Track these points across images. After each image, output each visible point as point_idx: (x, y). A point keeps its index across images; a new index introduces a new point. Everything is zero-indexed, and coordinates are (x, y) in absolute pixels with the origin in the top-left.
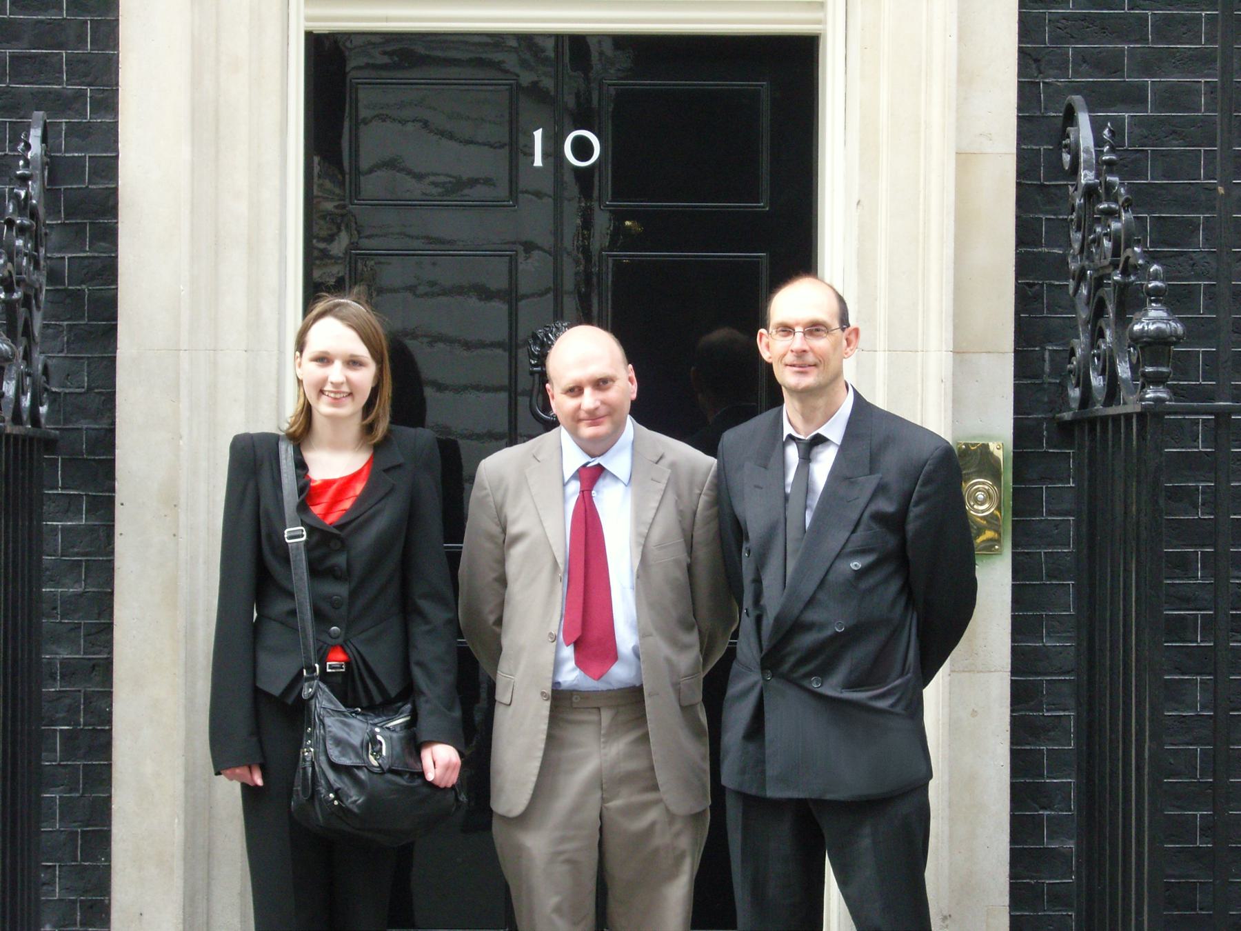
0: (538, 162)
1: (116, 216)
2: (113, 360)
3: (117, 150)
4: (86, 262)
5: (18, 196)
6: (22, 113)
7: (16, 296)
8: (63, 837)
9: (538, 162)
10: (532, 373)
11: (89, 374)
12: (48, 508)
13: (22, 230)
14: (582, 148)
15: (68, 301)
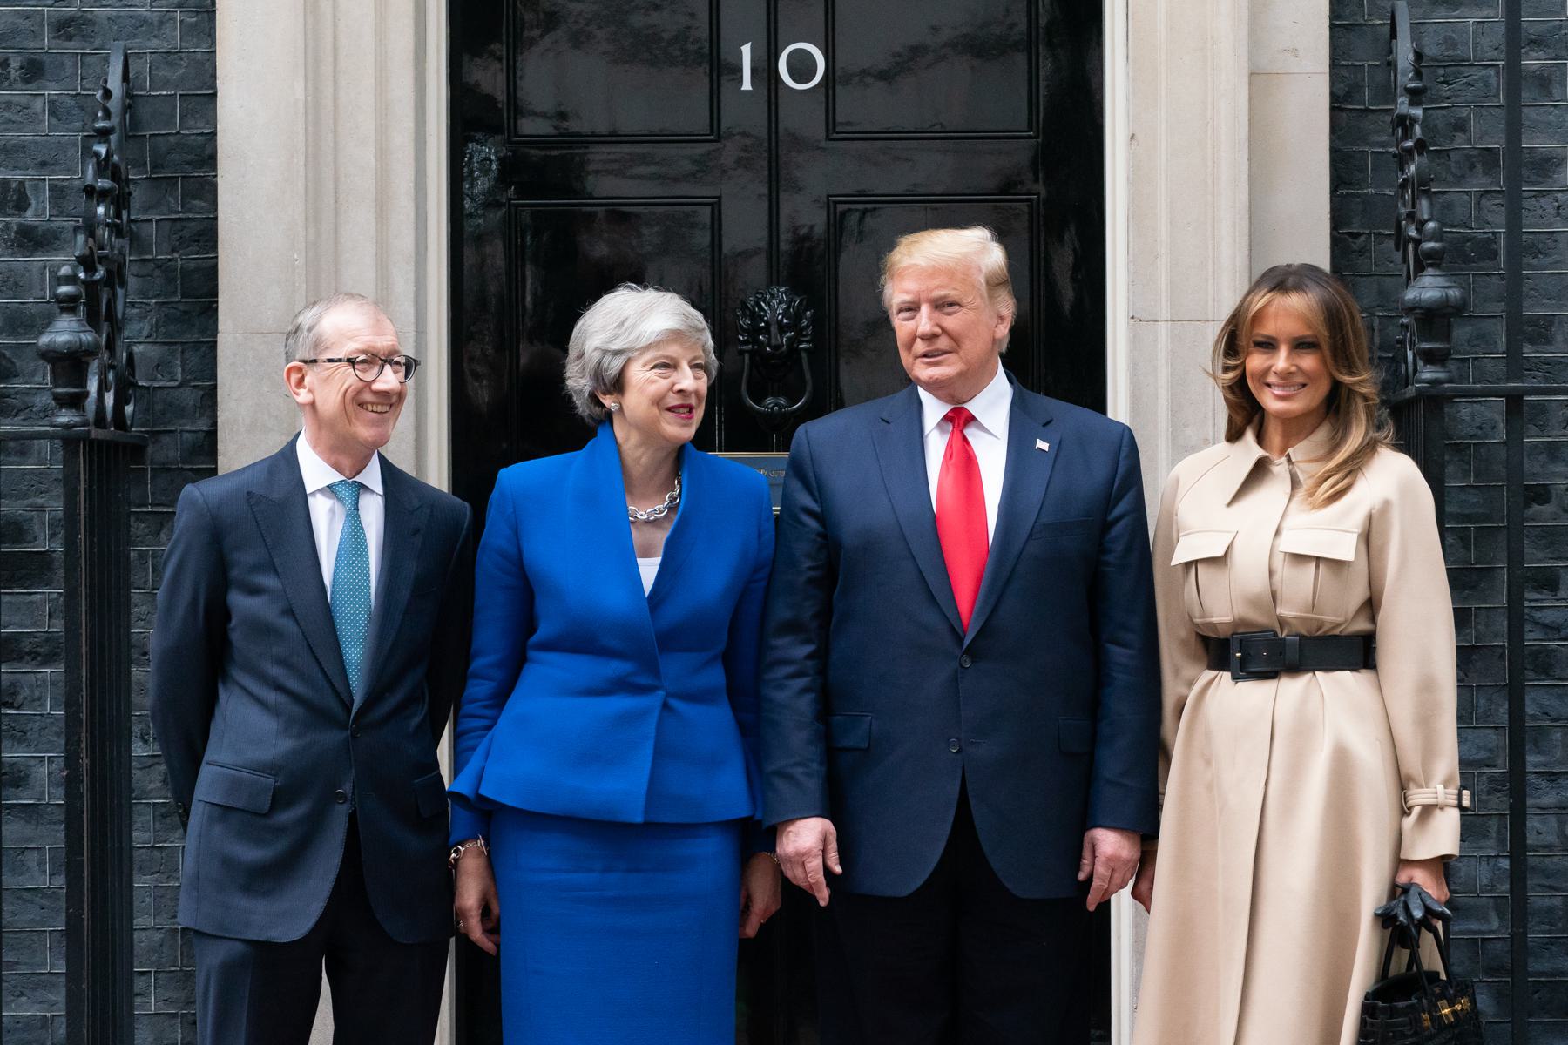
0: (747, 85)
1: (214, 168)
2: (213, 346)
3: (214, 86)
4: (178, 225)
5: (97, 155)
6: (97, 42)
7: (98, 276)
8: (158, 937)
9: (747, 85)
10: (742, 353)
11: (184, 362)
12: (138, 528)
13: (103, 195)
14: (802, 67)
15: (157, 273)
